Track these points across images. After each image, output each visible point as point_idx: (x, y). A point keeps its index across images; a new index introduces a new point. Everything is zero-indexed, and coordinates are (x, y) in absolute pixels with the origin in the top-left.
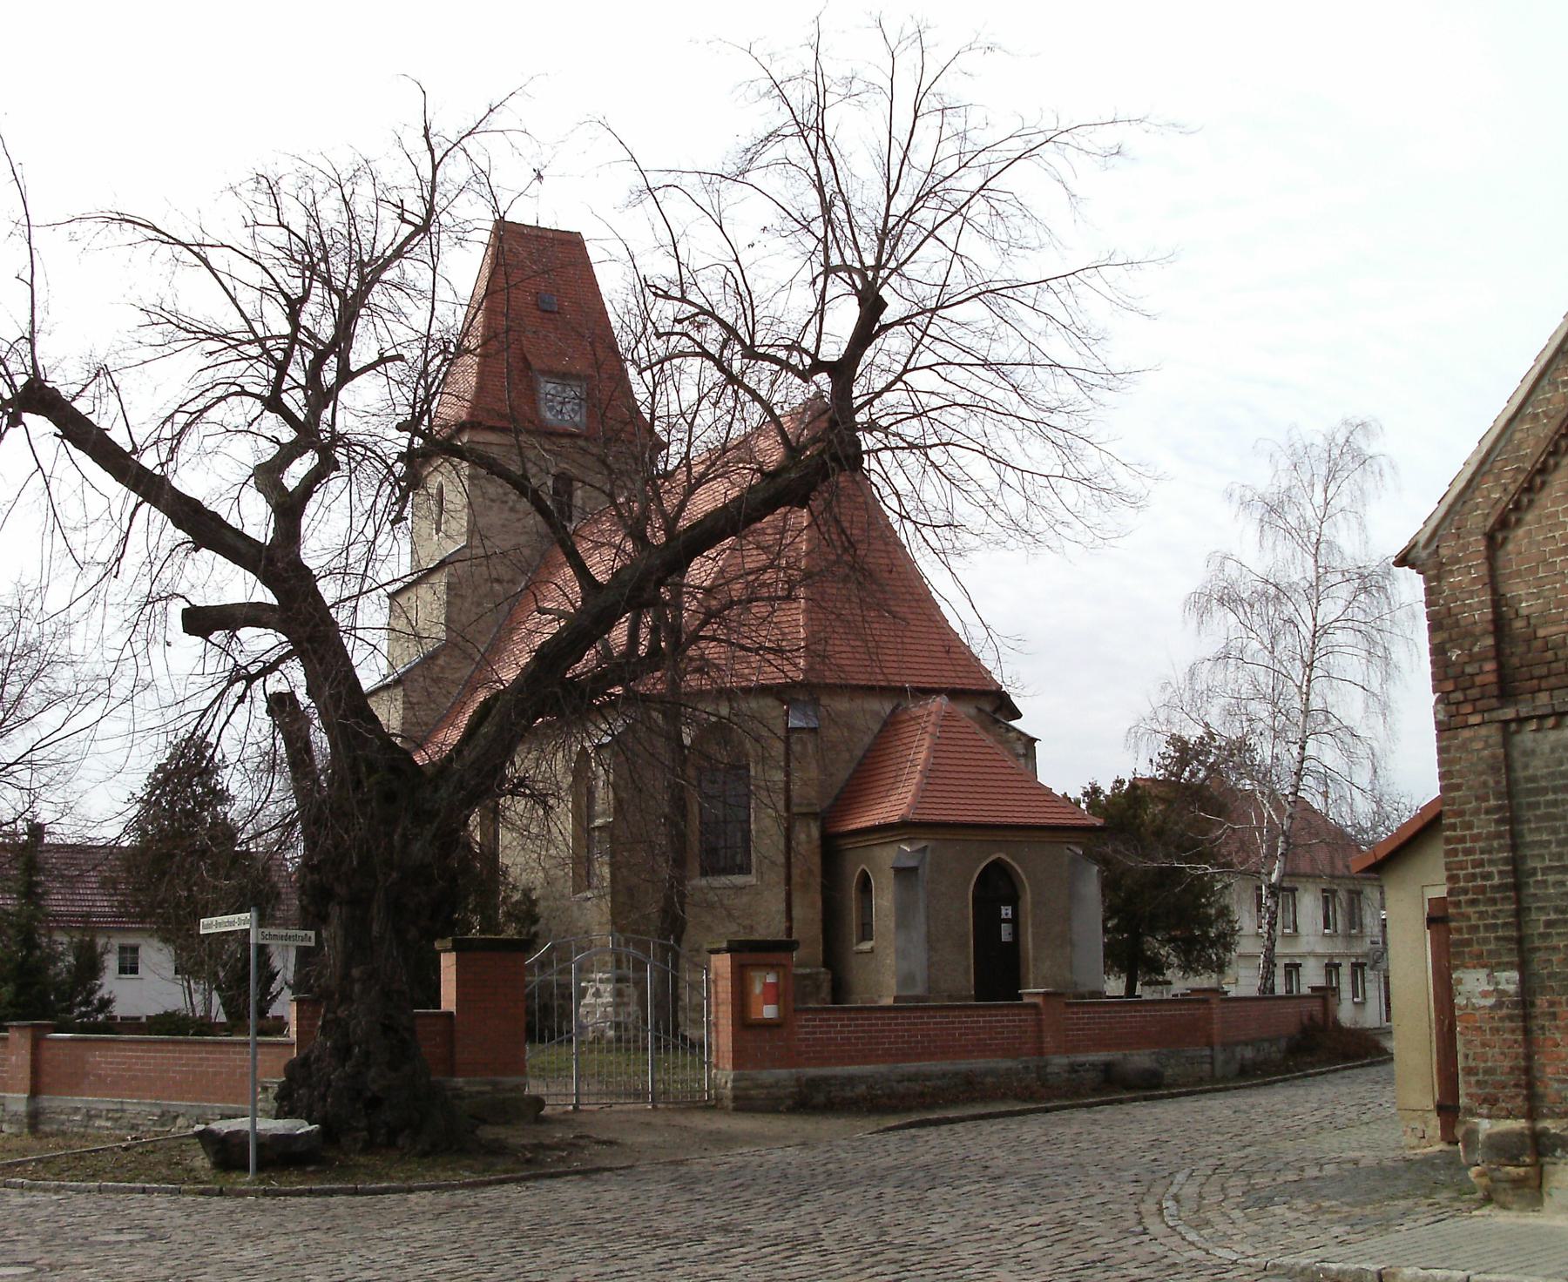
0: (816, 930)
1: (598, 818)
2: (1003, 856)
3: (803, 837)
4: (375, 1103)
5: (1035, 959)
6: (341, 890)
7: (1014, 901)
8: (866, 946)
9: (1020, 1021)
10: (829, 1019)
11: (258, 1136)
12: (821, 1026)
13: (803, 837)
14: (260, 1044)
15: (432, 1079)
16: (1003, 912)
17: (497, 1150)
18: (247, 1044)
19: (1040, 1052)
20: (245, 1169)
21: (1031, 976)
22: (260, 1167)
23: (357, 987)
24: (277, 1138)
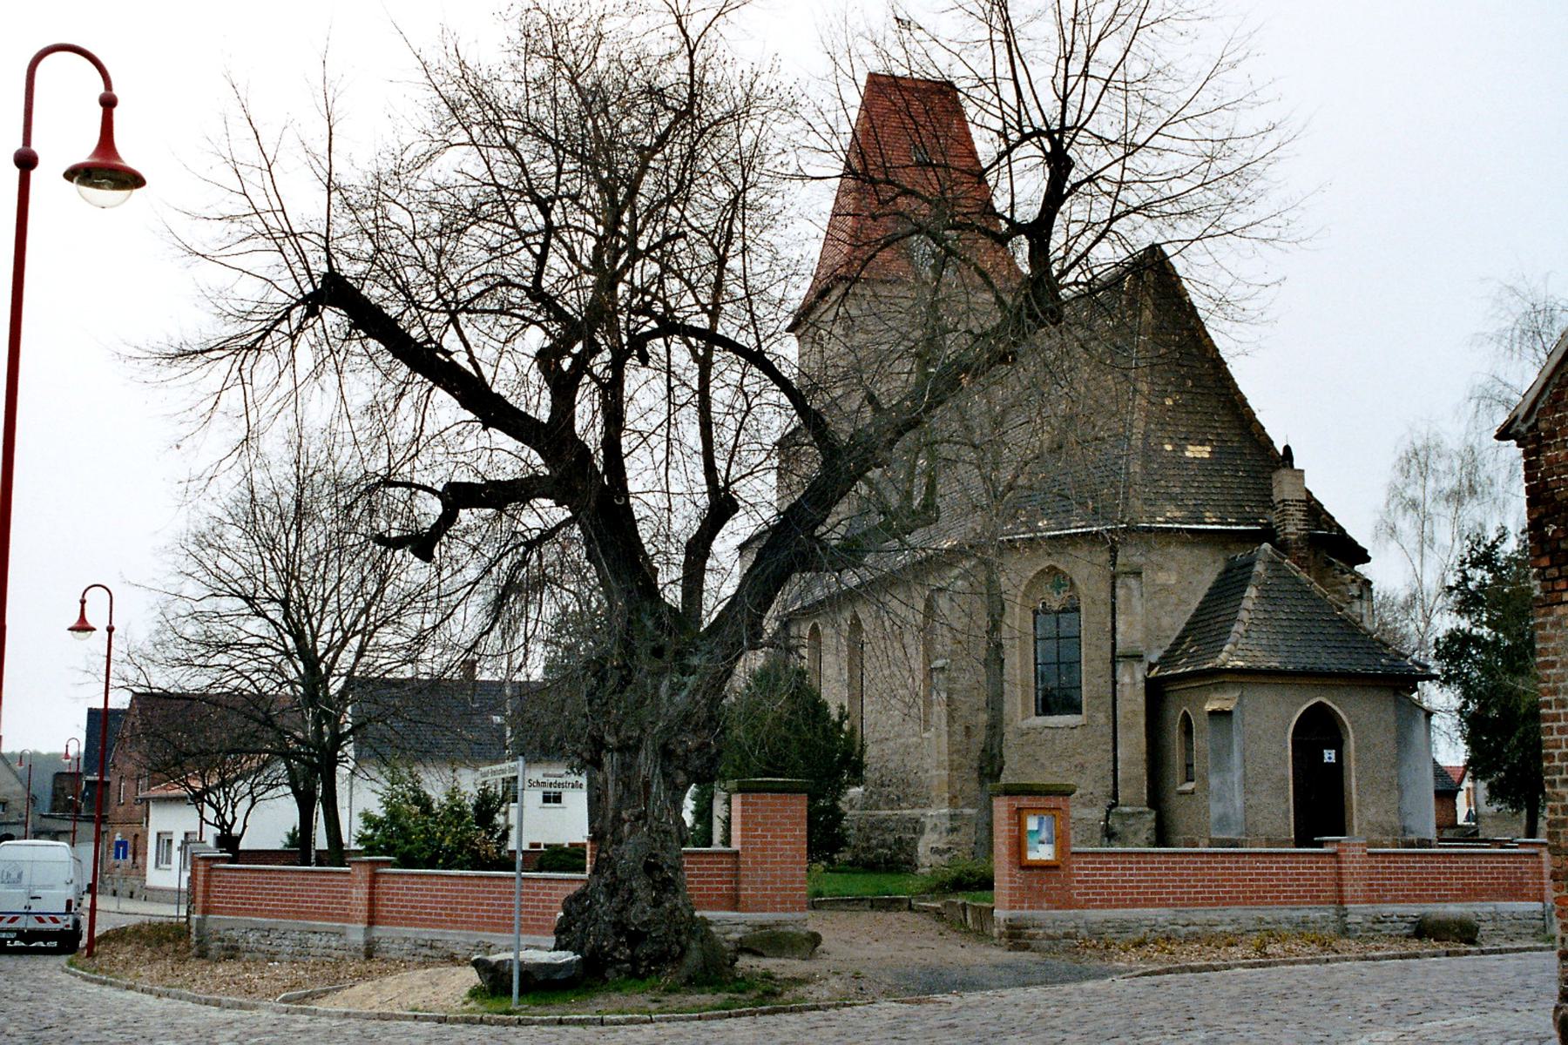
0: (1141, 771)
1: (937, 658)
2: (1324, 700)
3: (1127, 679)
4: (636, 938)
5: (1359, 804)
6: (610, 740)
7: (1338, 745)
8: (1189, 786)
9: (1318, 868)
10: (1109, 863)
11: (521, 964)
12: (1101, 869)
13: (1127, 679)
14: (524, 878)
15: (697, 914)
16: (1326, 756)
17: (742, 984)
18: (513, 878)
19: (1340, 901)
20: (509, 992)
21: (1355, 823)
22: (522, 993)
23: (626, 827)
24: (541, 967)
